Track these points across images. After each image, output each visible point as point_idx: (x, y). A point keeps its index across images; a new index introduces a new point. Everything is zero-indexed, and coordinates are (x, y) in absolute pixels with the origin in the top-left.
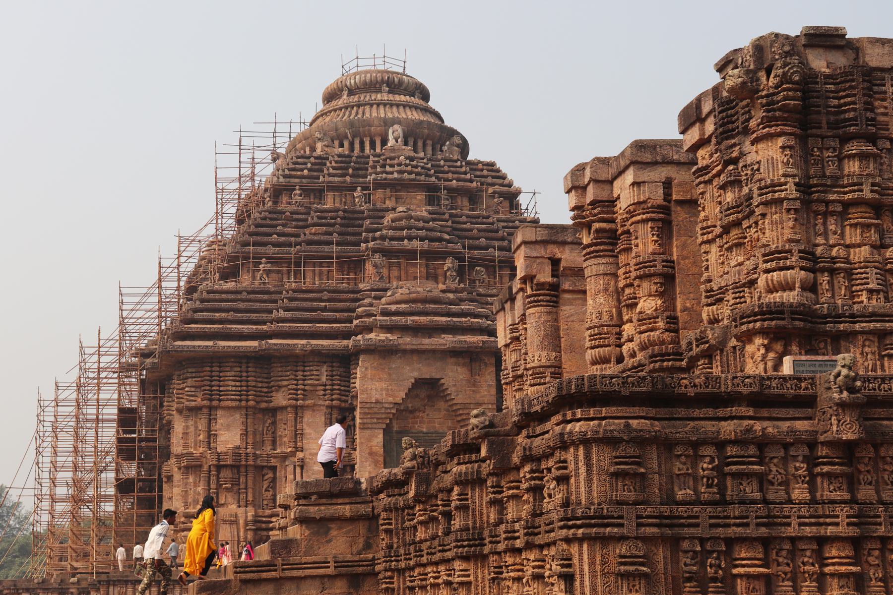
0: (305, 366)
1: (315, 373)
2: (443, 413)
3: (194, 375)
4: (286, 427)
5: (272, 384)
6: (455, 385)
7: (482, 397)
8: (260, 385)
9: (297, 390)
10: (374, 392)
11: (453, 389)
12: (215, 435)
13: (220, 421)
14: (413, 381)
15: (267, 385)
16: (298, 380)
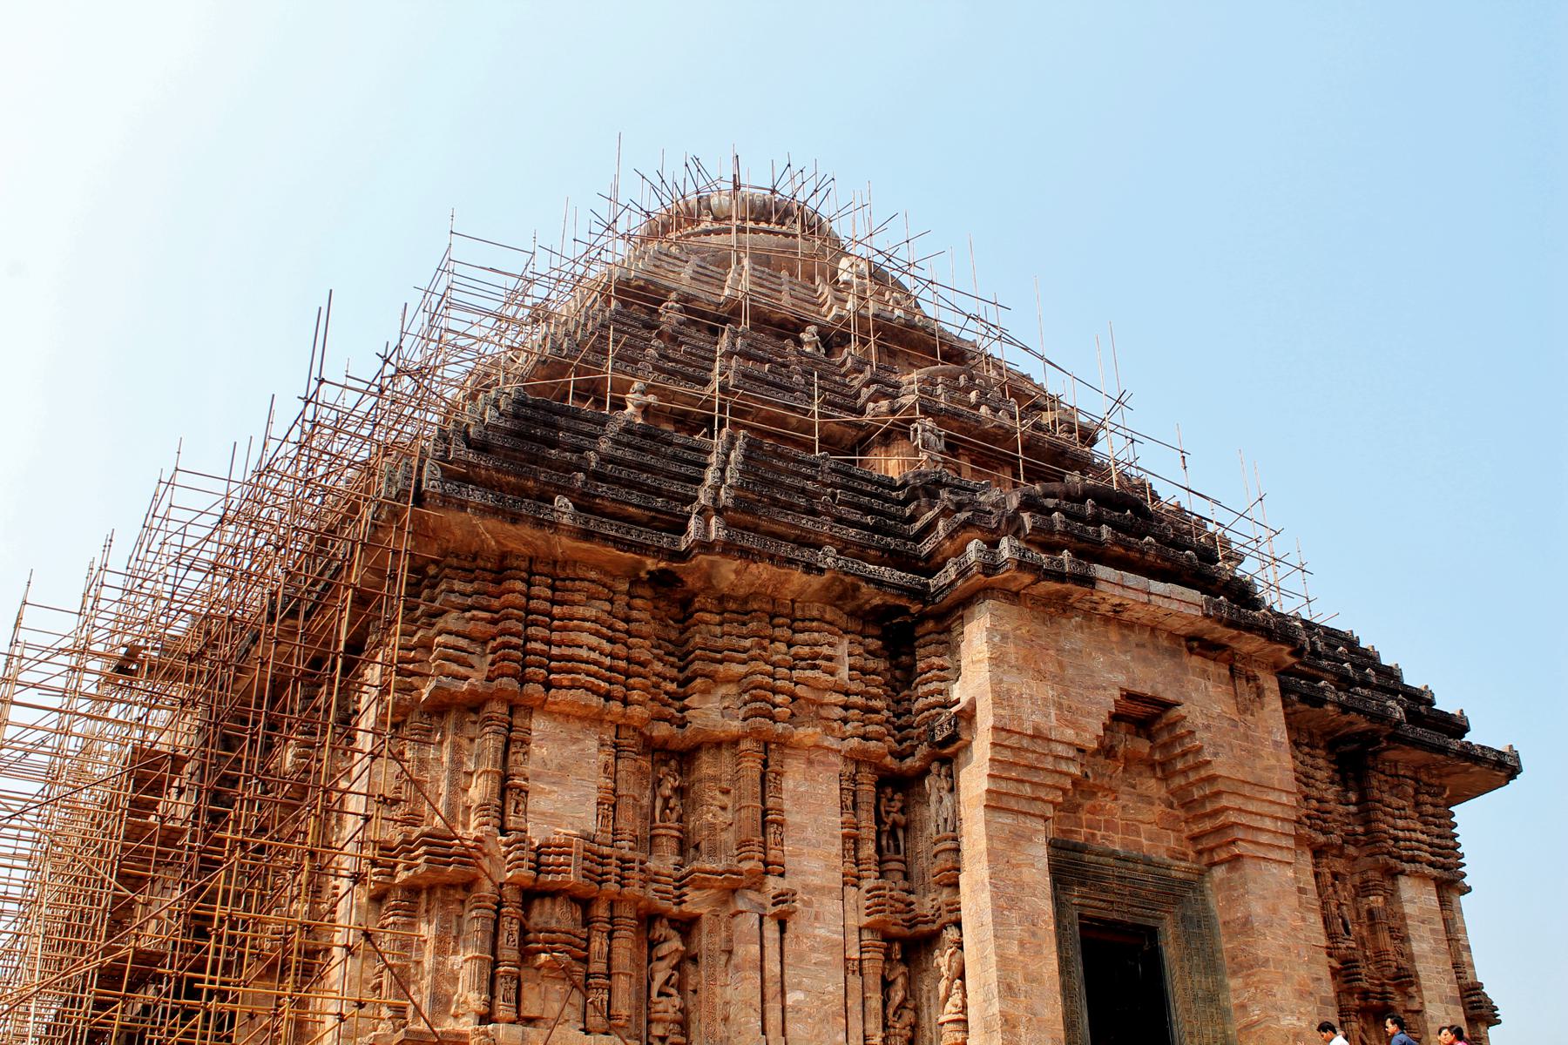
0: (794, 631)
1: (826, 650)
2: (1160, 808)
3: (469, 601)
4: (725, 800)
5: (697, 665)
6: (1207, 727)
7: (1267, 769)
8: (658, 667)
9: (775, 691)
10: (1027, 706)
11: (1206, 735)
12: (523, 791)
13: (539, 751)
14: (1117, 695)
15: (675, 672)
16: (774, 665)
